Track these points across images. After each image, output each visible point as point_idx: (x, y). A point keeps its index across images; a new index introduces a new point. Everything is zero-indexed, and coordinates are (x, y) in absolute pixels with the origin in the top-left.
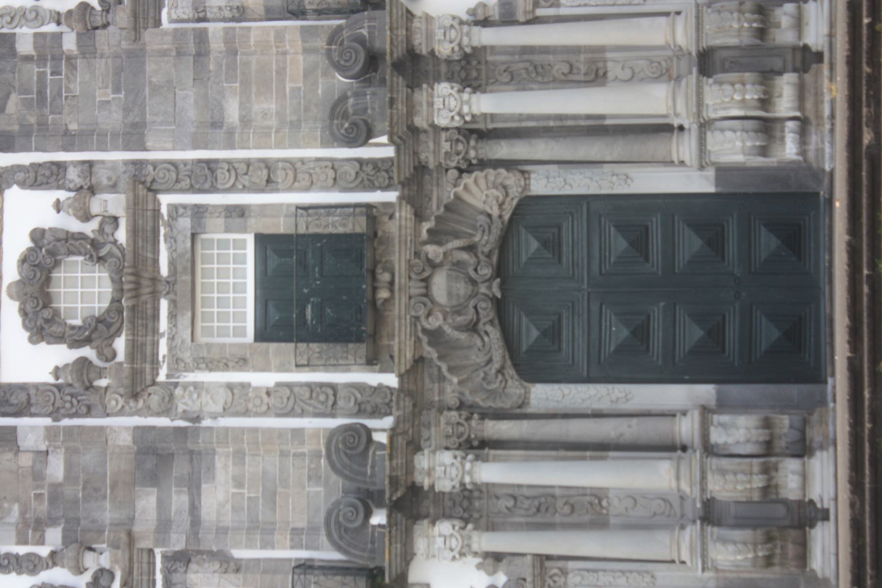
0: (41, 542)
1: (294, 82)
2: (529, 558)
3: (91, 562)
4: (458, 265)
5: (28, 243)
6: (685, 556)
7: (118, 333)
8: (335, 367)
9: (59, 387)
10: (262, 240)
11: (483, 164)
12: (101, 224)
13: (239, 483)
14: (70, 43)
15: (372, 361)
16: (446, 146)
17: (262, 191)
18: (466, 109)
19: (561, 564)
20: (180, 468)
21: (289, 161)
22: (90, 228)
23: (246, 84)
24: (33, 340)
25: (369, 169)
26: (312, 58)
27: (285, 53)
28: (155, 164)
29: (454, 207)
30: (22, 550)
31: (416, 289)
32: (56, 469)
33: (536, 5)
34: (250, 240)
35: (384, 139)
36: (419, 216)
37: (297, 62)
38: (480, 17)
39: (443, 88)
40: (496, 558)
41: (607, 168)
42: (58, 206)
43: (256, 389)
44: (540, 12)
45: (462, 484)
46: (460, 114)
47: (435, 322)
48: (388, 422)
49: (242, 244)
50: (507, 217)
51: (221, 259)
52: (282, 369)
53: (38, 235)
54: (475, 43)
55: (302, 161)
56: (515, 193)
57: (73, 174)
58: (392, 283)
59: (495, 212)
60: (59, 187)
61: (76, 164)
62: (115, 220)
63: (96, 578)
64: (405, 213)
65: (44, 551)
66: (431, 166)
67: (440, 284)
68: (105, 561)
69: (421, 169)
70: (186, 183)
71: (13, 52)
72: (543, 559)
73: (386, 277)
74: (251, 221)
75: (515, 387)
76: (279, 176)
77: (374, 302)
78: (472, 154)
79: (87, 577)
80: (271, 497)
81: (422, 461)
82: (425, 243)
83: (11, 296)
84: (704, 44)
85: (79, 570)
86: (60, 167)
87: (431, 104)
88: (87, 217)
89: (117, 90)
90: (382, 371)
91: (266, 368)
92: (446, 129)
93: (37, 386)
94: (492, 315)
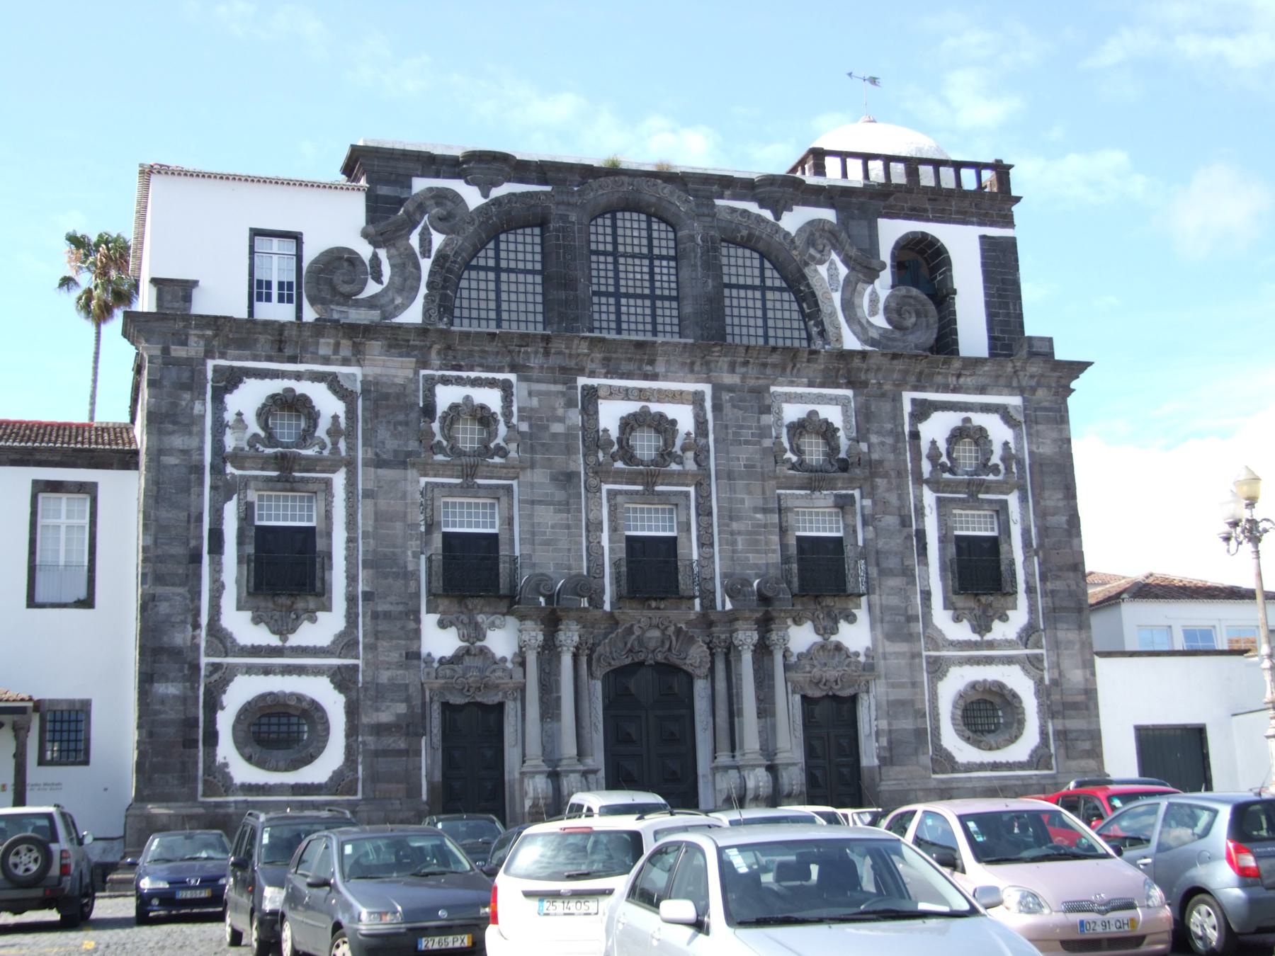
0: (521, 419)
1: (752, 558)
2: (523, 680)
3: (512, 447)
4: (663, 642)
5: (670, 417)
6: (528, 763)
7: (626, 463)
8: (611, 578)
9: (598, 431)
10: (674, 539)
11: (712, 655)
12: (679, 456)
13: (553, 527)
14: (767, 443)
15: (619, 599)
16: (723, 637)
17: (698, 540)
18: (746, 647)
19: (519, 697)
20: (560, 495)
21: (713, 556)
22: (677, 449)
23: (750, 533)
24: (622, 418)
25: (711, 596)
26: (764, 568)
27: (766, 553)
28: (709, 485)
29: (691, 640)
30: (515, 409)
31: (654, 622)
32: (557, 428)
33: (793, 682)
34: (673, 534)
35: (729, 606)
36: (688, 623)
37: (761, 560)
38: (787, 654)
39: (756, 636)
40: (523, 664)
41: (711, 719)
42: (688, 434)
43: (600, 537)
44: (789, 684)
45: (561, 646)
46: (743, 644)
47: (637, 632)
48: (587, 605)
49: (671, 529)
50: (685, 668)
51: (664, 520)
52: (611, 550)
53: (674, 422)
54: (775, 652)
55: (713, 562)
56: (698, 672)
57: (702, 441)
58: (658, 608)
59: (688, 662)
60: (696, 434)
61: (708, 442)
62: (681, 463)
63: (502, 448)
64: (692, 616)
65: (514, 420)
66: (714, 629)
67: (656, 633)
68: (513, 454)
69: (711, 624)
70: (701, 501)
71: (761, 412)
72: (523, 689)
73: (662, 606)
74: (684, 534)
75: (599, 673)
76: (706, 550)
77: (648, 599)
78: (719, 650)
79: (503, 444)
80: (547, 543)
81: (575, 627)
82: (675, 625)
83: (643, 407)
84: (780, 767)
85: (506, 440)
86: (706, 436)
87: (747, 630)
88: (684, 449)
89: (745, 466)
90: (612, 603)
91: (611, 541)
92: (731, 637)
93: (597, 420)
94: (636, 660)
